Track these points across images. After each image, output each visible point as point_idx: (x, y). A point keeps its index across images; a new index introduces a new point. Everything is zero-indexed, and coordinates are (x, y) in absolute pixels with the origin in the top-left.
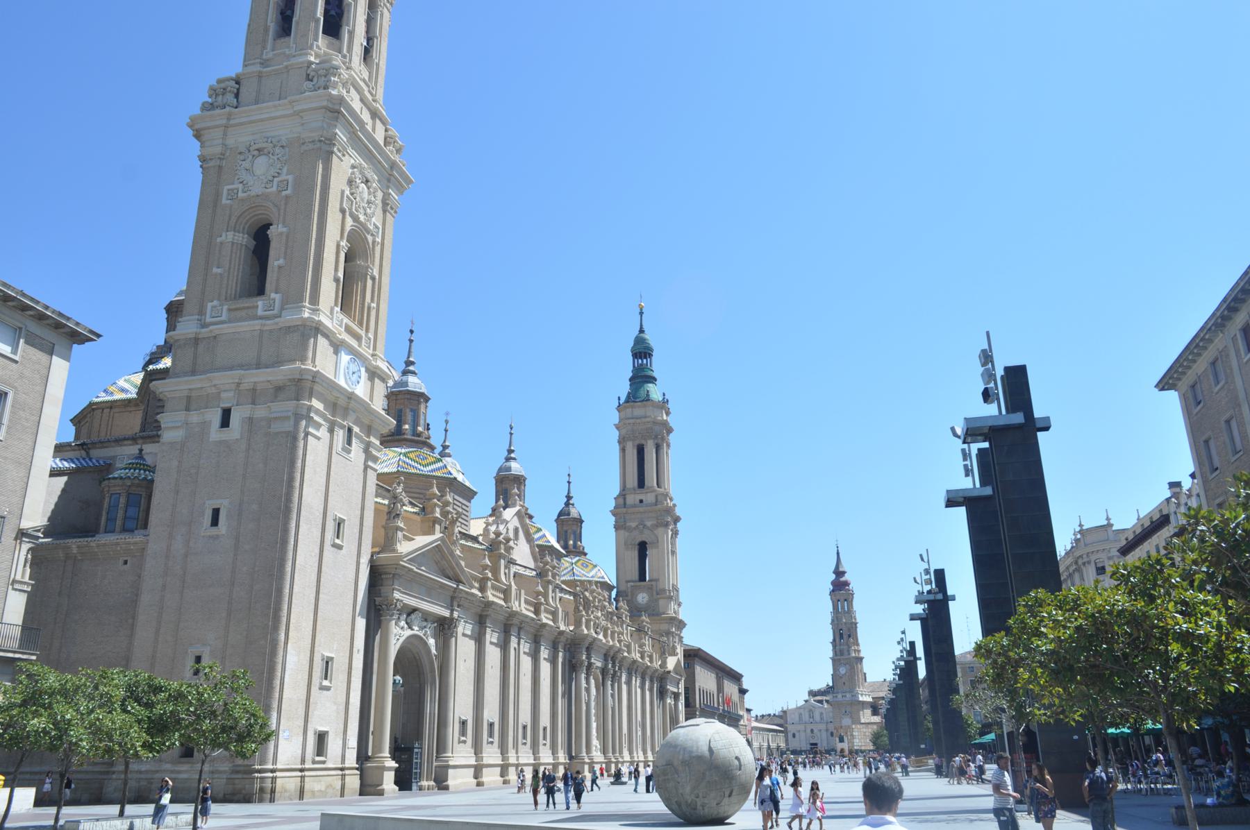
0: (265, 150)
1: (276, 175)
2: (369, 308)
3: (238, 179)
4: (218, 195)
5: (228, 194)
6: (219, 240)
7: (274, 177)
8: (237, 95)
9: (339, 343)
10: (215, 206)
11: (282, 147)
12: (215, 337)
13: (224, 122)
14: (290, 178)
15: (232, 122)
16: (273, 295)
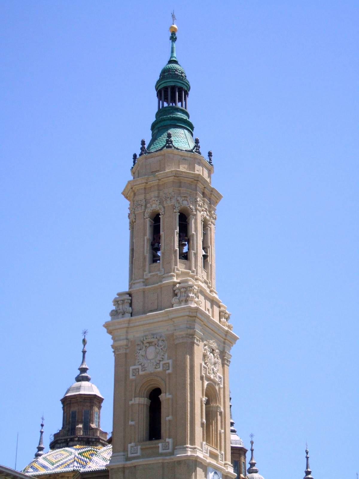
0: (153, 343)
1: (161, 359)
2: (220, 434)
3: (138, 362)
4: (127, 372)
5: (133, 372)
6: (130, 403)
7: (160, 361)
8: (131, 305)
9: (207, 465)
10: (126, 379)
11: (163, 340)
12: (135, 466)
13: (127, 325)
14: (170, 361)
15: (131, 325)
16: (167, 440)
